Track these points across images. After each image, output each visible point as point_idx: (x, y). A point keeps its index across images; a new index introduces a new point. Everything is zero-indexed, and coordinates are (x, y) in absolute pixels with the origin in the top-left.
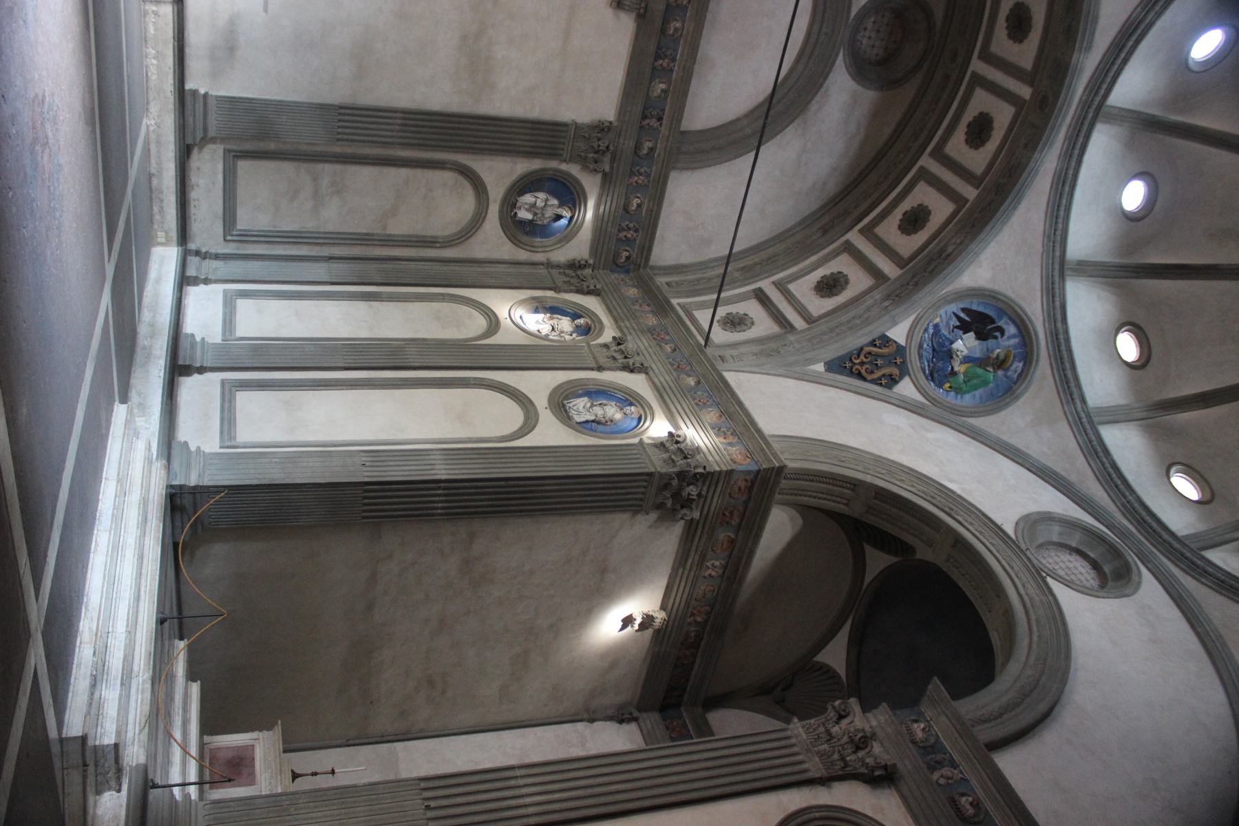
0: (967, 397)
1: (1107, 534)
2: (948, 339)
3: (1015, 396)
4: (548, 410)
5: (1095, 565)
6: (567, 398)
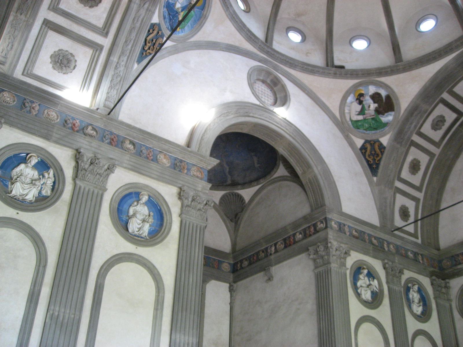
0: (186, 28)
1: (263, 66)
2: (173, 4)
3: (206, 18)
4: (138, 247)
5: (263, 82)
6: (127, 230)
